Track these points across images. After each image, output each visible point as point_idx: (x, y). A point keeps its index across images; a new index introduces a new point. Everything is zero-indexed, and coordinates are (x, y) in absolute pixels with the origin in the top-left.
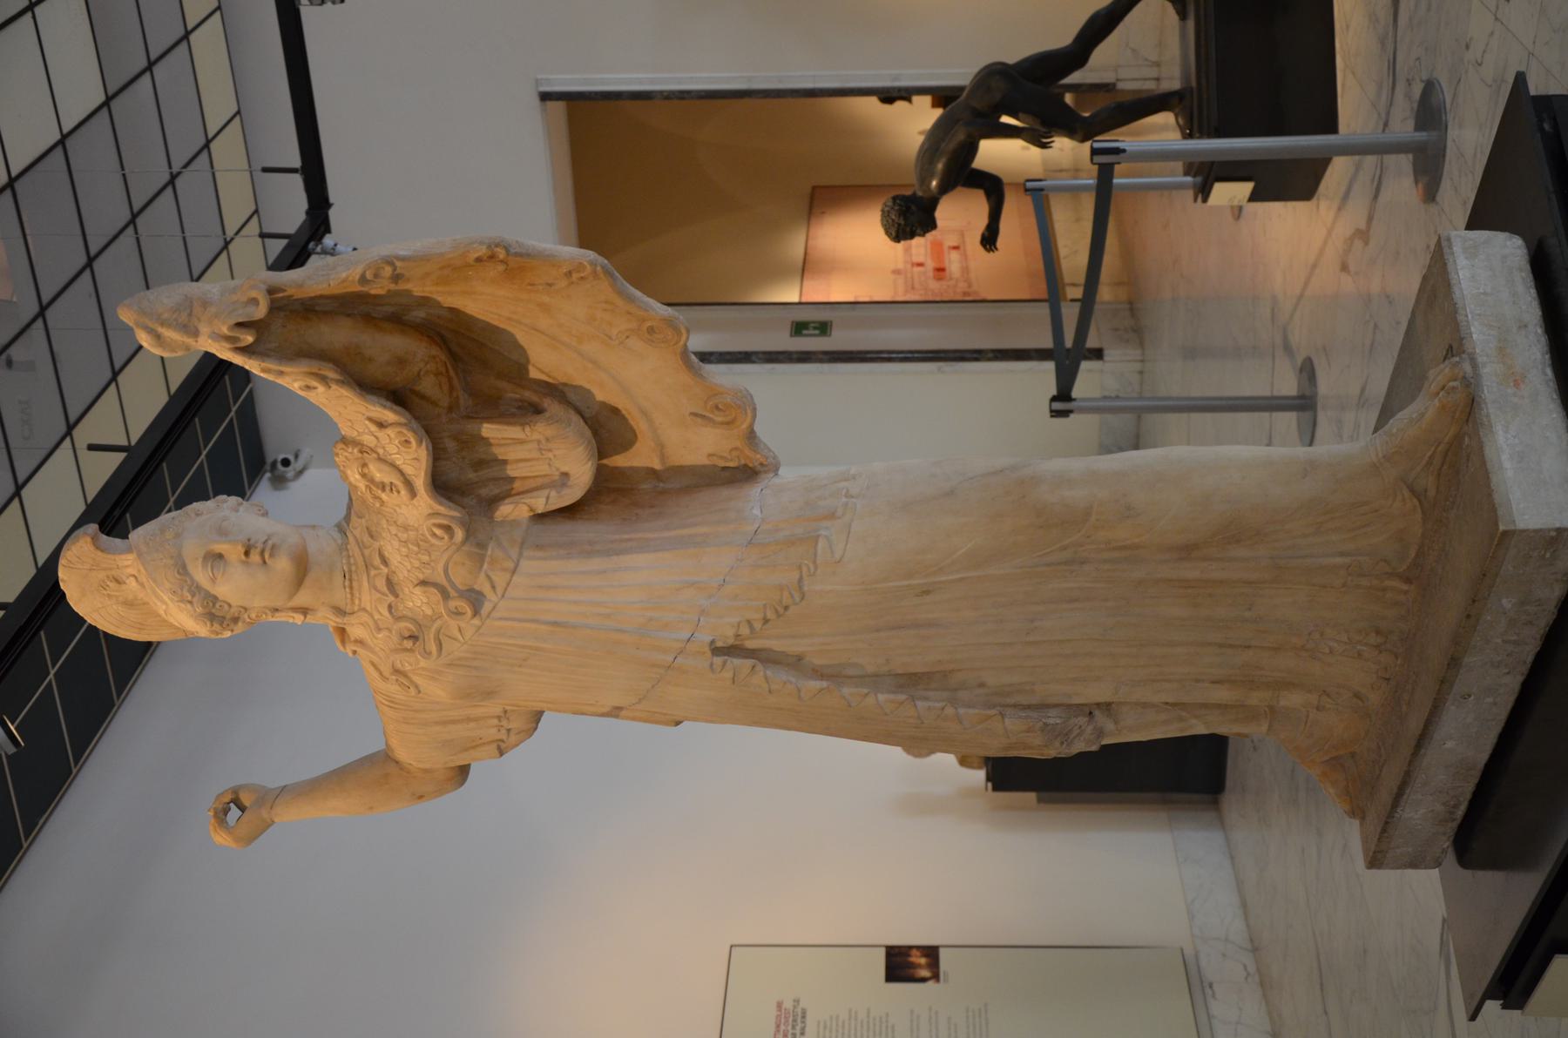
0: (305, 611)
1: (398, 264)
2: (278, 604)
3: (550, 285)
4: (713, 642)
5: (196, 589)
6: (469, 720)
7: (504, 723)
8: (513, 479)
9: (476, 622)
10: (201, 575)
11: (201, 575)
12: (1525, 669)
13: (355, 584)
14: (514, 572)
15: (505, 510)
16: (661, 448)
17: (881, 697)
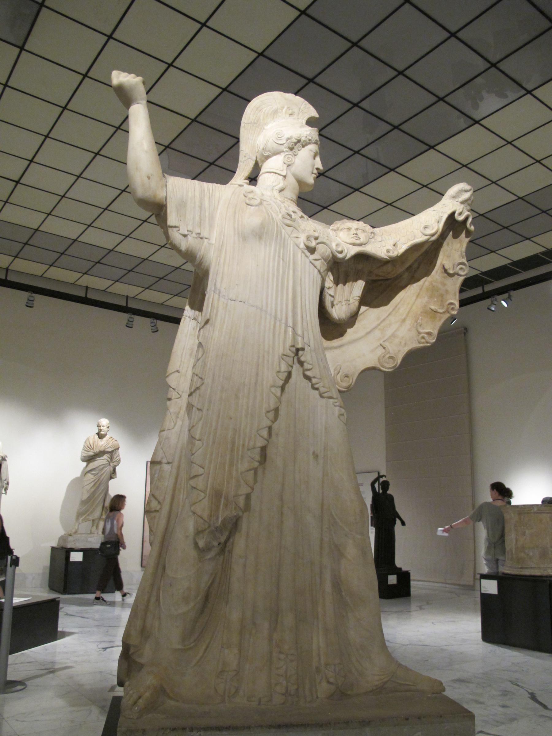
0: (285, 177)
2: (293, 169)
3: (421, 325)
4: (303, 349)
7: (194, 235)
8: (337, 285)
9: (302, 246)
14: (319, 271)
15: (331, 277)
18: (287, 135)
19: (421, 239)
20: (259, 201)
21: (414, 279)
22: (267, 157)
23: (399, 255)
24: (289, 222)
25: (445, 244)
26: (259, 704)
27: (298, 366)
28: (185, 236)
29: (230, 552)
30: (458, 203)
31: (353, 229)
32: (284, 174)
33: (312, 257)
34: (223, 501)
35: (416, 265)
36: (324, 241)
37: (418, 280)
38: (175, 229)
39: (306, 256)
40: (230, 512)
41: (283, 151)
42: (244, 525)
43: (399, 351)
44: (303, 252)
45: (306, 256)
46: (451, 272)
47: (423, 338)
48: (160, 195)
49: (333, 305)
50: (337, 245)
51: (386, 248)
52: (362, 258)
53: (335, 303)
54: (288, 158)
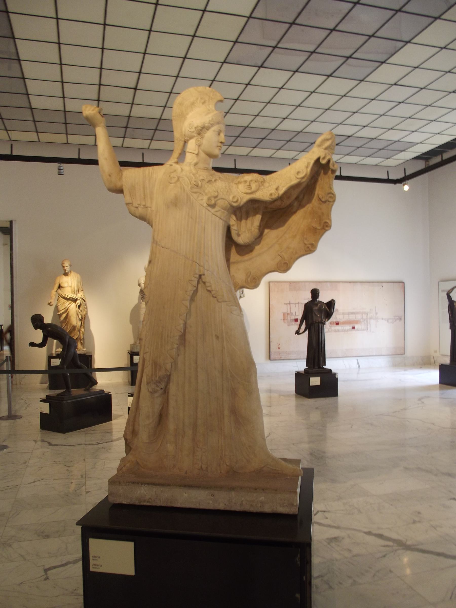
0: (197, 155)
1: (332, 203)
2: (202, 147)
4: (204, 275)
5: (212, 125)
6: (145, 196)
7: (142, 206)
8: (241, 220)
9: (205, 205)
10: (215, 128)
11: (215, 128)
12: (228, 508)
13: (205, 171)
14: (220, 218)
15: (234, 217)
16: (238, 262)
17: (182, 325)
18: (195, 125)
19: (295, 181)
20: (176, 178)
21: (301, 206)
22: (188, 140)
23: (280, 195)
24: (195, 190)
25: (319, 179)
26: (186, 473)
27: (202, 284)
28: (137, 207)
29: (168, 392)
30: (323, 150)
31: (248, 181)
32: (196, 152)
33: (213, 210)
34: (158, 366)
35: (301, 197)
36: (223, 197)
37: (304, 206)
38: (130, 205)
39: (209, 210)
40: (161, 373)
41: (194, 136)
42: (174, 378)
43: (291, 258)
44: (207, 209)
45: (209, 210)
46: (323, 200)
47: (308, 247)
48: (119, 184)
49: (239, 235)
50: (234, 197)
51: (270, 192)
52: (253, 202)
53: (240, 233)
54: (198, 141)
